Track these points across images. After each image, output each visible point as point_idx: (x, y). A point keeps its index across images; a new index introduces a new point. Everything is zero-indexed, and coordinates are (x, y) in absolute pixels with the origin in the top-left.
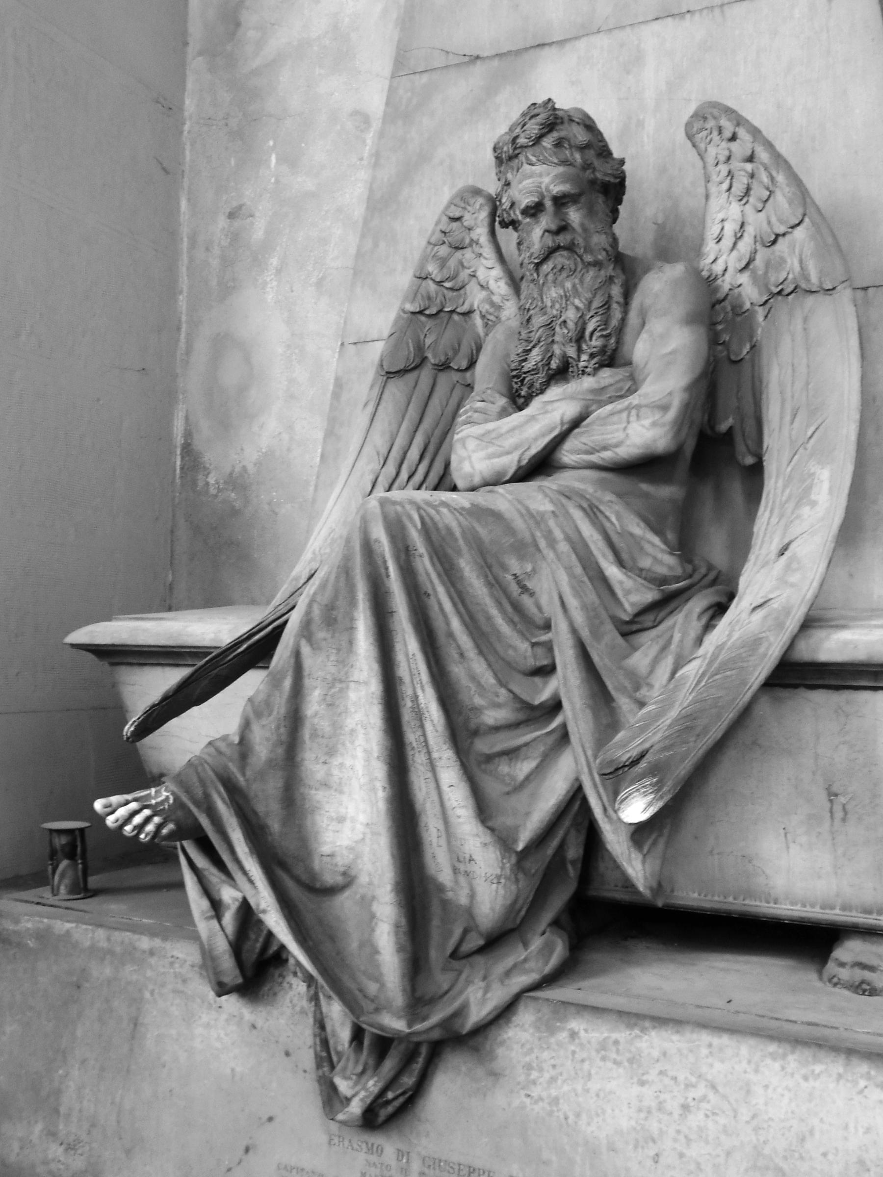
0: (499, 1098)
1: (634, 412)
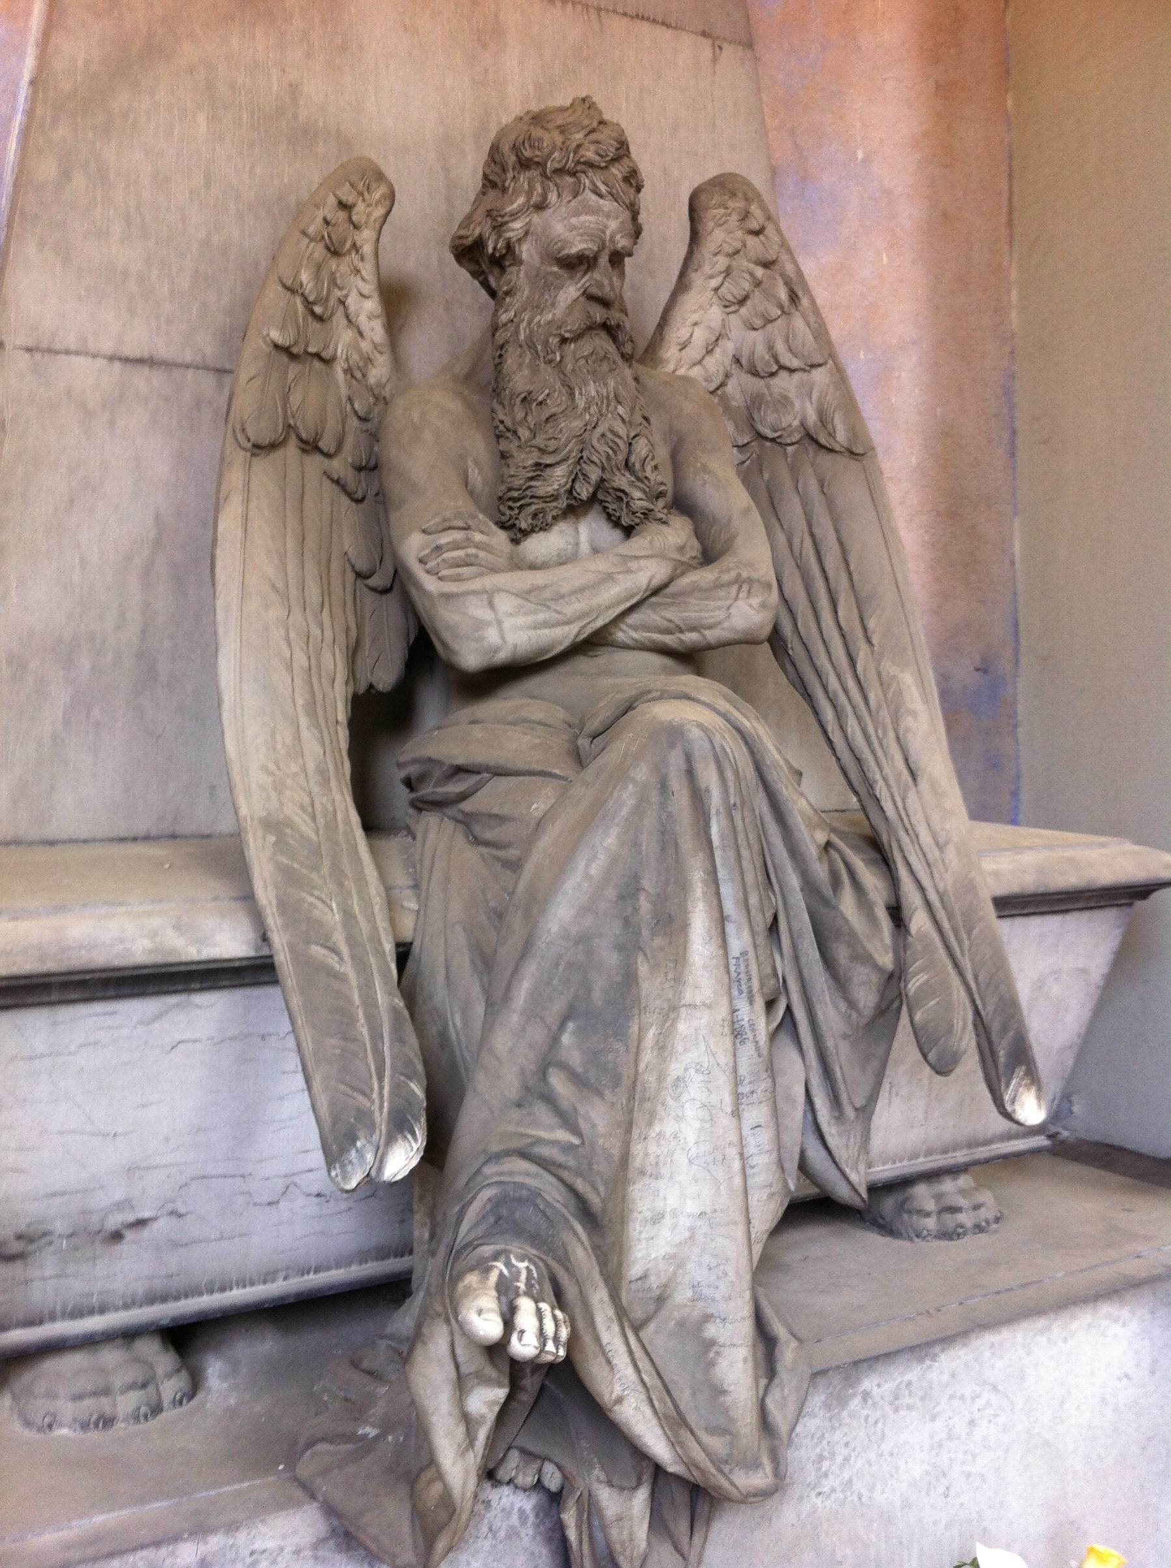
1: (745, 587)
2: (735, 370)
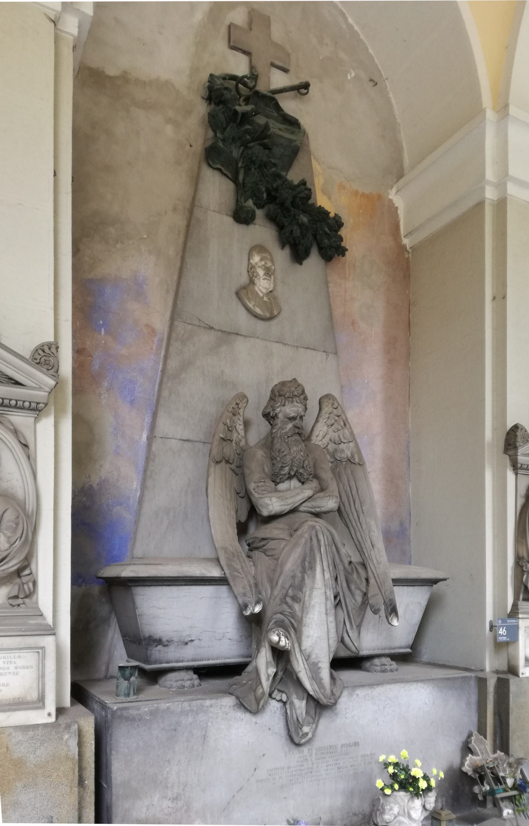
0: (339, 721)
2: (330, 442)
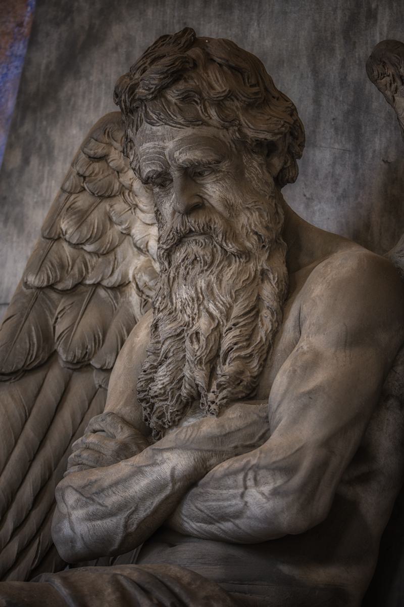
1: (251, 475)
